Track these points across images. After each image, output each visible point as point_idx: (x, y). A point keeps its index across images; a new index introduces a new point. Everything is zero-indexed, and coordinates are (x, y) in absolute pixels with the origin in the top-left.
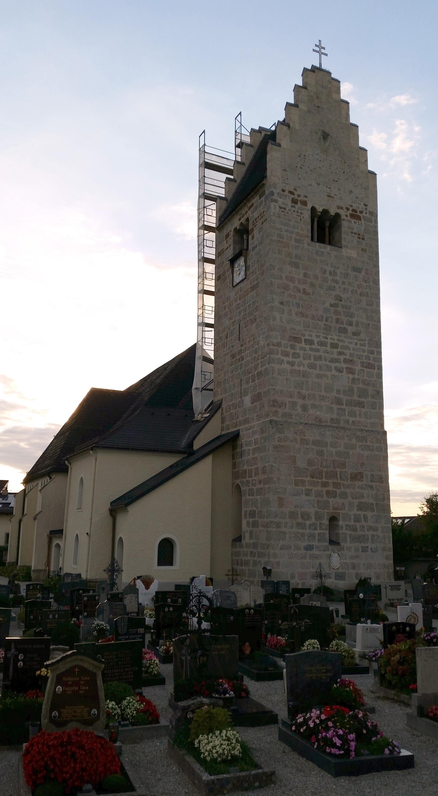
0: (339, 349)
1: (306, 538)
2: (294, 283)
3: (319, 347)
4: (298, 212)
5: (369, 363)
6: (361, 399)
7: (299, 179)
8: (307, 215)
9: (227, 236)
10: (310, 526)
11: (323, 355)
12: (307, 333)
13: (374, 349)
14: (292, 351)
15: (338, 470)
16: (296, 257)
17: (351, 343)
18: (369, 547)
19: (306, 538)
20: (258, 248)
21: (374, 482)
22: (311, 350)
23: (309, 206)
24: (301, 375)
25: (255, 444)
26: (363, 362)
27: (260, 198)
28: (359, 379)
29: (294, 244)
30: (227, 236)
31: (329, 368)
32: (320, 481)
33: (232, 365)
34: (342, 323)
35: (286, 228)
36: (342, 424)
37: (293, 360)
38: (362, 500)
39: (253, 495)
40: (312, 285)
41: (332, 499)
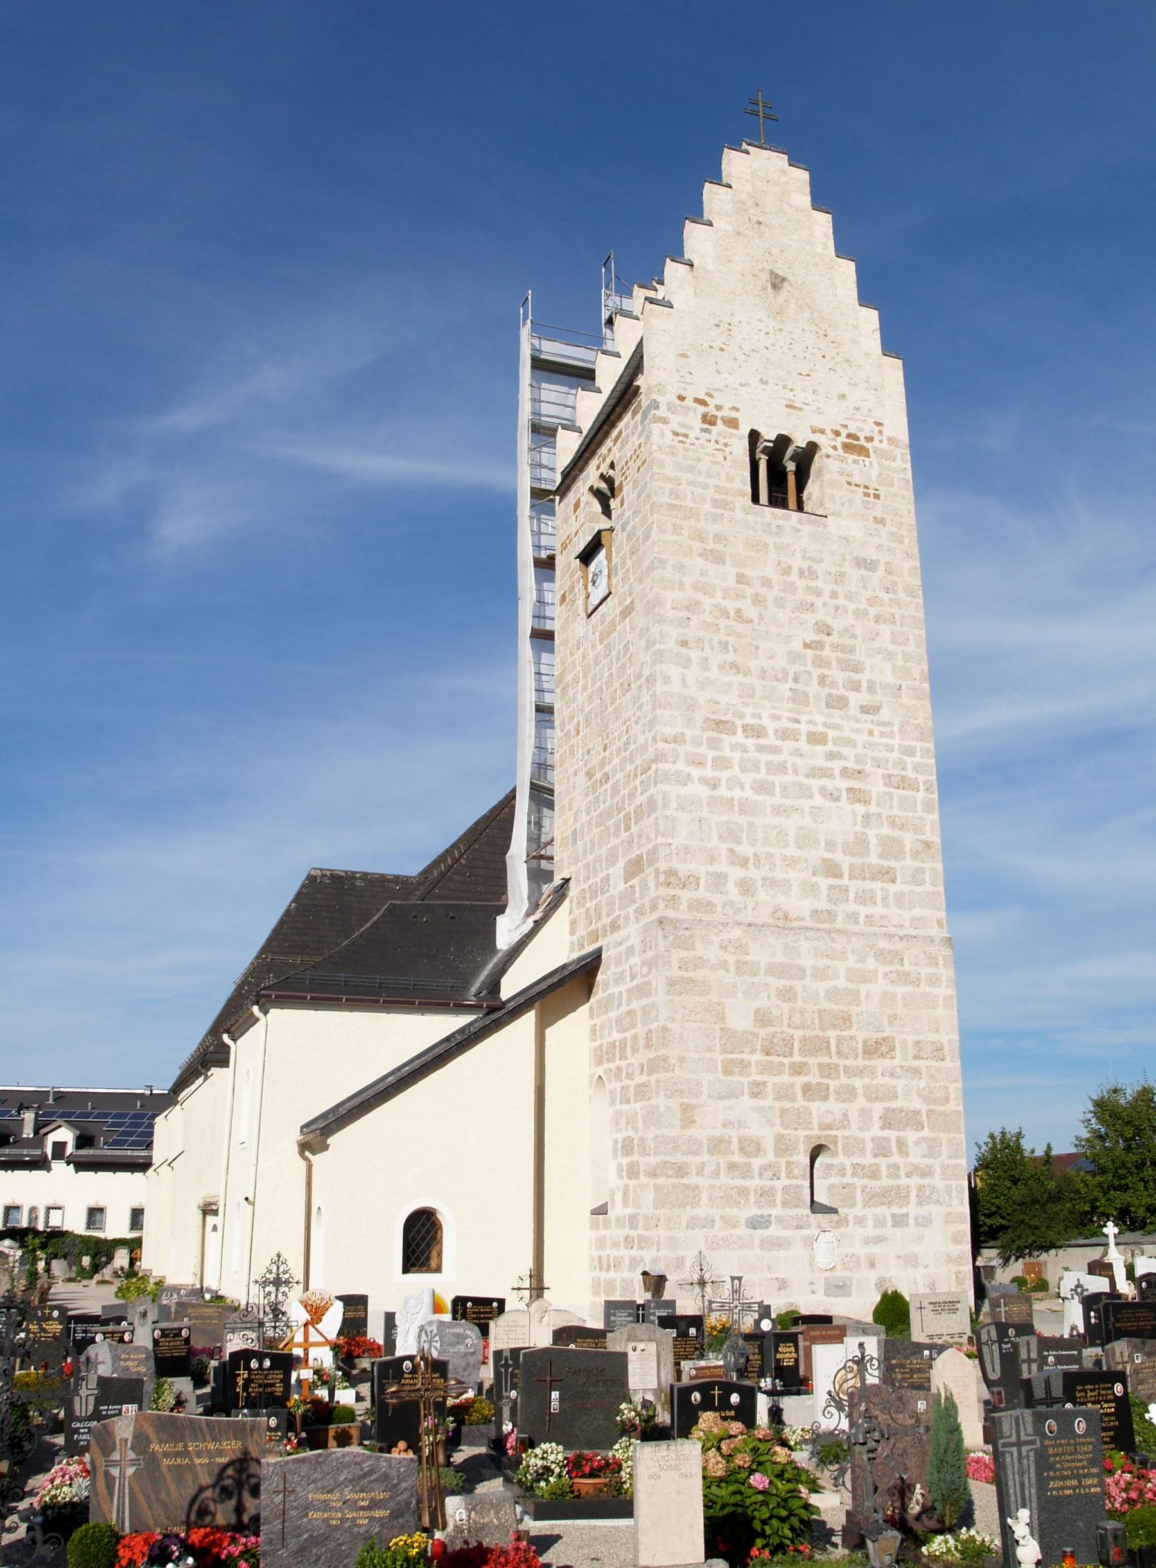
0: (830, 747)
1: (752, 1198)
2: (712, 596)
3: (779, 743)
4: (717, 442)
5: (903, 778)
6: (886, 863)
7: (719, 372)
8: (740, 448)
9: (577, 506)
10: (763, 1169)
11: (791, 760)
12: (748, 711)
13: (913, 743)
14: (711, 754)
15: (832, 1034)
16: (718, 538)
17: (857, 731)
18: (911, 1216)
19: (752, 1198)
20: (632, 524)
21: (922, 1058)
22: (760, 749)
23: (745, 431)
24: (736, 808)
26: (890, 776)
27: (633, 417)
28: (879, 815)
29: (713, 510)
30: (577, 506)
31: (805, 792)
32: (786, 1061)
33: (587, 795)
34: (834, 685)
35: (690, 477)
36: (840, 923)
37: (716, 774)
38: (894, 1104)
39: (628, 1102)
40: (758, 600)
41: (818, 1103)
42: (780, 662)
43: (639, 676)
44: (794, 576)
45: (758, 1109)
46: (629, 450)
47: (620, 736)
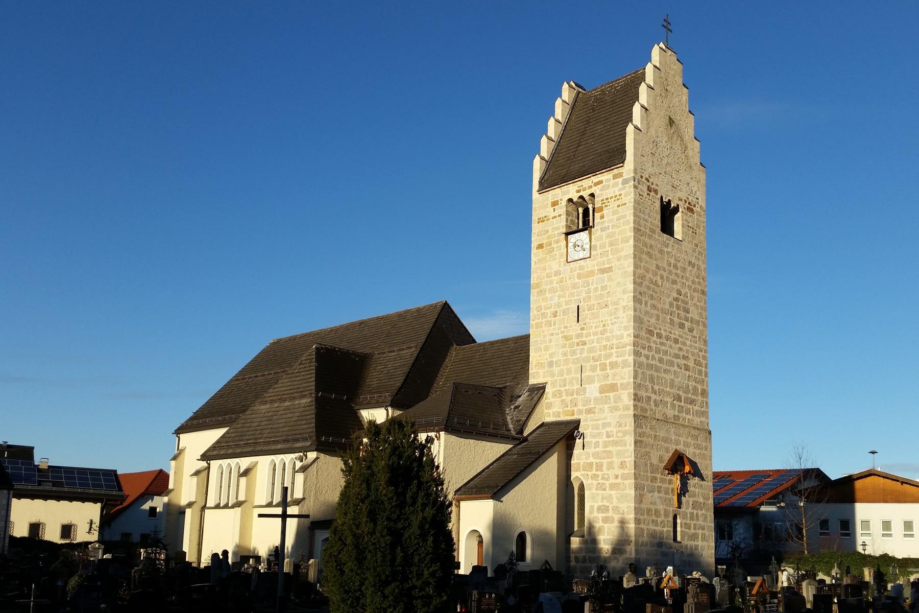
8: (658, 205)
16: (651, 246)
25: (608, 436)
27: (615, 177)
31: (671, 364)
38: (696, 499)
39: (604, 490)
40: (662, 277)
42: (667, 307)
43: (616, 304)
44: (672, 268)
45: (660, 498)
46: (609, 193)
47: (596, 327)
